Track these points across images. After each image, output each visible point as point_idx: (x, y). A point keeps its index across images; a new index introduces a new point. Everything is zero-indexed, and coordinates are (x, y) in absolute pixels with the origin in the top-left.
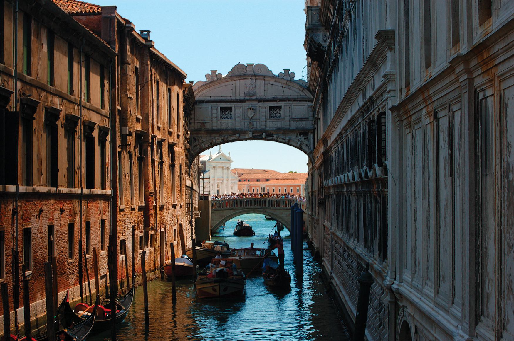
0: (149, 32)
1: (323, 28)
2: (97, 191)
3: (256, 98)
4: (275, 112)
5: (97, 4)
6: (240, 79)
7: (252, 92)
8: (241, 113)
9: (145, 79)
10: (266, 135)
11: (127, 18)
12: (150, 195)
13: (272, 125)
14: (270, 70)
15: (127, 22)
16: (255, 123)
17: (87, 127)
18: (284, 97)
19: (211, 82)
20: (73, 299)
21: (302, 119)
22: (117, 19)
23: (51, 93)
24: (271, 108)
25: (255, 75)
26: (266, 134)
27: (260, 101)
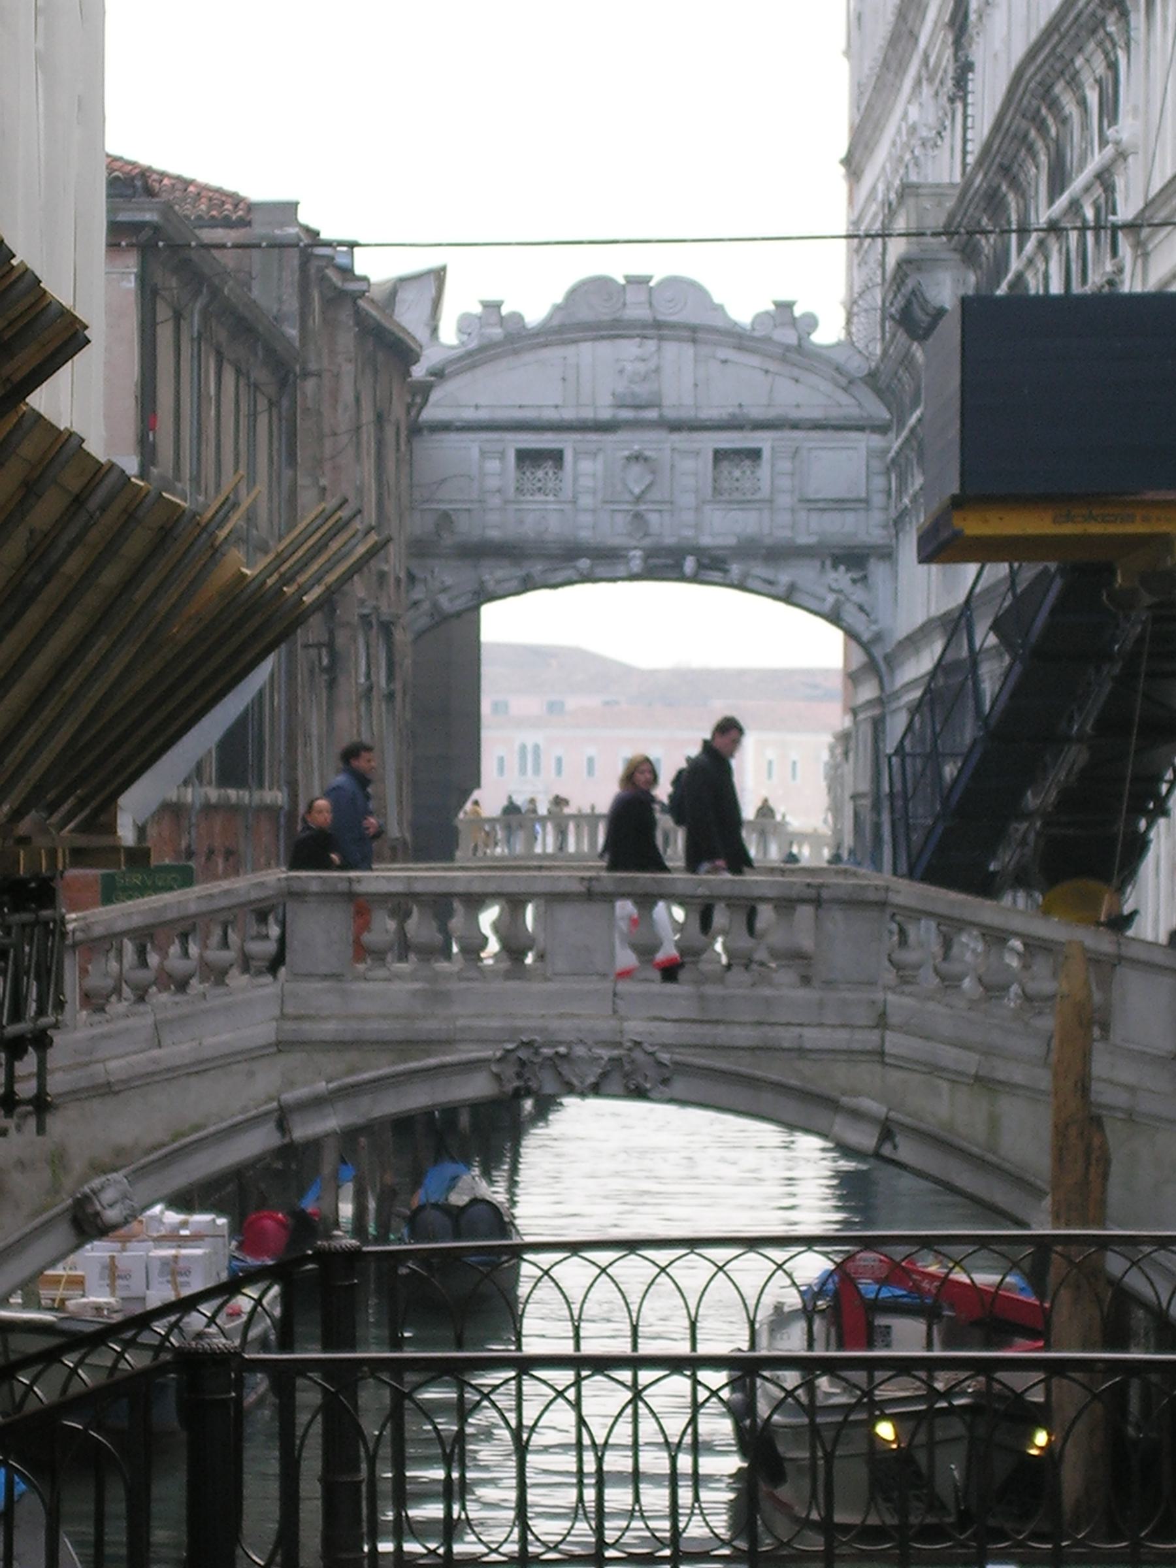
1: (957, 256)
3: (661, 416)
4: (737, 473)
6: (595, 339)
7: (643, 390)
10: (701, 566)
14: (717, 299)
16: (653, 518)
18: (771, 414)
19: (482, 349)
24: (720, 456)
25: (658, 325)
27: (676, 427)
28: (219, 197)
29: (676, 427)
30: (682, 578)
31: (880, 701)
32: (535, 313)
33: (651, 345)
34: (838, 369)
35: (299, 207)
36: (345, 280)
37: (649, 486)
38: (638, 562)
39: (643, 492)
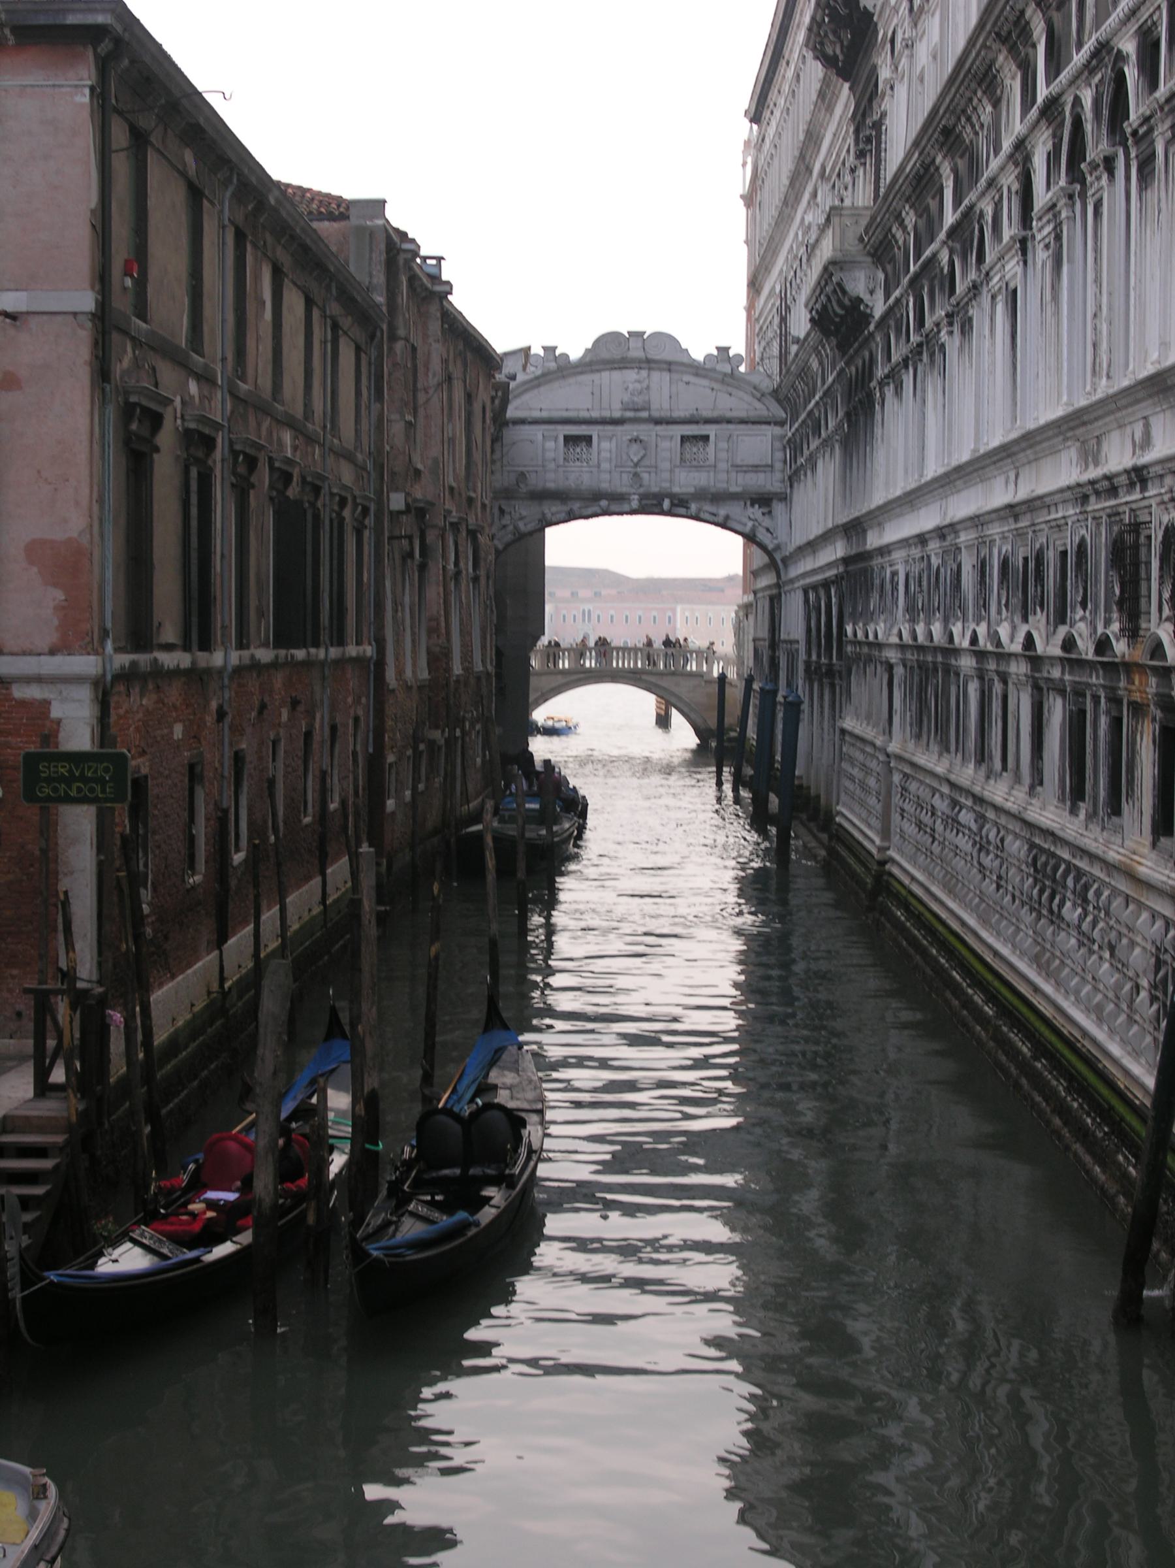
0: (440, 259)
1: (869, 259)
2: (352, 650)
4: (695, 450)
6: (612, 369)
7: (639, 400)
8: (614, 450)
10: (673, 505)
11: (402, 228)
13: (685, 482)
14: (684, 346)
15: (403, 235)
16: (645, 476)
17: (337, 498)
18: (715, 414)
19: (544, 375)
21: (757, 466)
22: (386, 230)
23: (278, 421)
24: (684, 439)
25: (648, 361)
27: (658, 422)
28: (327, 199)
29: (658, 422)
30: (663, 513)
31: (778, 586)
32: (575, 353)
33: (644, 373)
34: (755, 388)
35: (387, 205)
36: (433, 284)
37: (642, 458)
39: (639, 461)
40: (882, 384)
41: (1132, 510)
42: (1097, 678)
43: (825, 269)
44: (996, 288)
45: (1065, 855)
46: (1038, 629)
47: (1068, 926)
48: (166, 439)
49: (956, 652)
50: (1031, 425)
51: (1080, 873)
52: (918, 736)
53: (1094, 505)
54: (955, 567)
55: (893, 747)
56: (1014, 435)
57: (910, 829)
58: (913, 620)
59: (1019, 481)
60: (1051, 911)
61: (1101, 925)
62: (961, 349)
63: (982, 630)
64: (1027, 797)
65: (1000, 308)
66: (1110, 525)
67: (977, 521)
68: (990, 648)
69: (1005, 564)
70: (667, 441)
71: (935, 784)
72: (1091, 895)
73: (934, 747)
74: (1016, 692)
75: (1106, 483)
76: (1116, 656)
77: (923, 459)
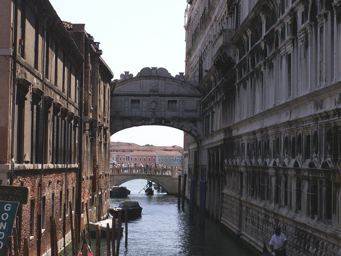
0: (99, 43)
3: (158, 94)
4: (172, 105)
5: (68, 21)
6: (146, 79)
9: (95, 79)
10: (165, 122)
11: (89, 33)
12: (97, 168)
13: (169, 114)
18: (179, 94)
19: (125, 80)
20: (61, 249)
24: (169, 101)
25: (158, 77)
26: (165, 121)
27: (161, 96)
29: (161, 96)
33: (157, 80)
34: (192, 85)
38: (154, 121)
40: (239, 84)
41: (334, 122)
42: (322, 175)
43: (220, 48)
44: (283, 54)
45: (310, 232)
46: (298, 160)
47: (311, 254)
48: (29, 96)
49: (268, 168)
50: (296, 96)
51: (315, 238)
52: (252, 195)
53: (320, 121)
54: (267, 141)
55: (243, 198)
56: (290, 100)
57: (249, 224)
58: (250, 158)
59: (292, 114)
60: (304, 249)
61: (324, 253)
62: (269, 73)
63: (278, 160)
64: (295, 213)
65: (284, 60)
66: (326, 127)
67: (276, 127)
68: (280, 166)
69: (286, 140)
70: (164, 102)
71: (260, 210)
72: (320, 244)
73: (258, 198)
74: (290, 180)
75: (325, 114)
76: (330, 168)
77: (254, 107)
